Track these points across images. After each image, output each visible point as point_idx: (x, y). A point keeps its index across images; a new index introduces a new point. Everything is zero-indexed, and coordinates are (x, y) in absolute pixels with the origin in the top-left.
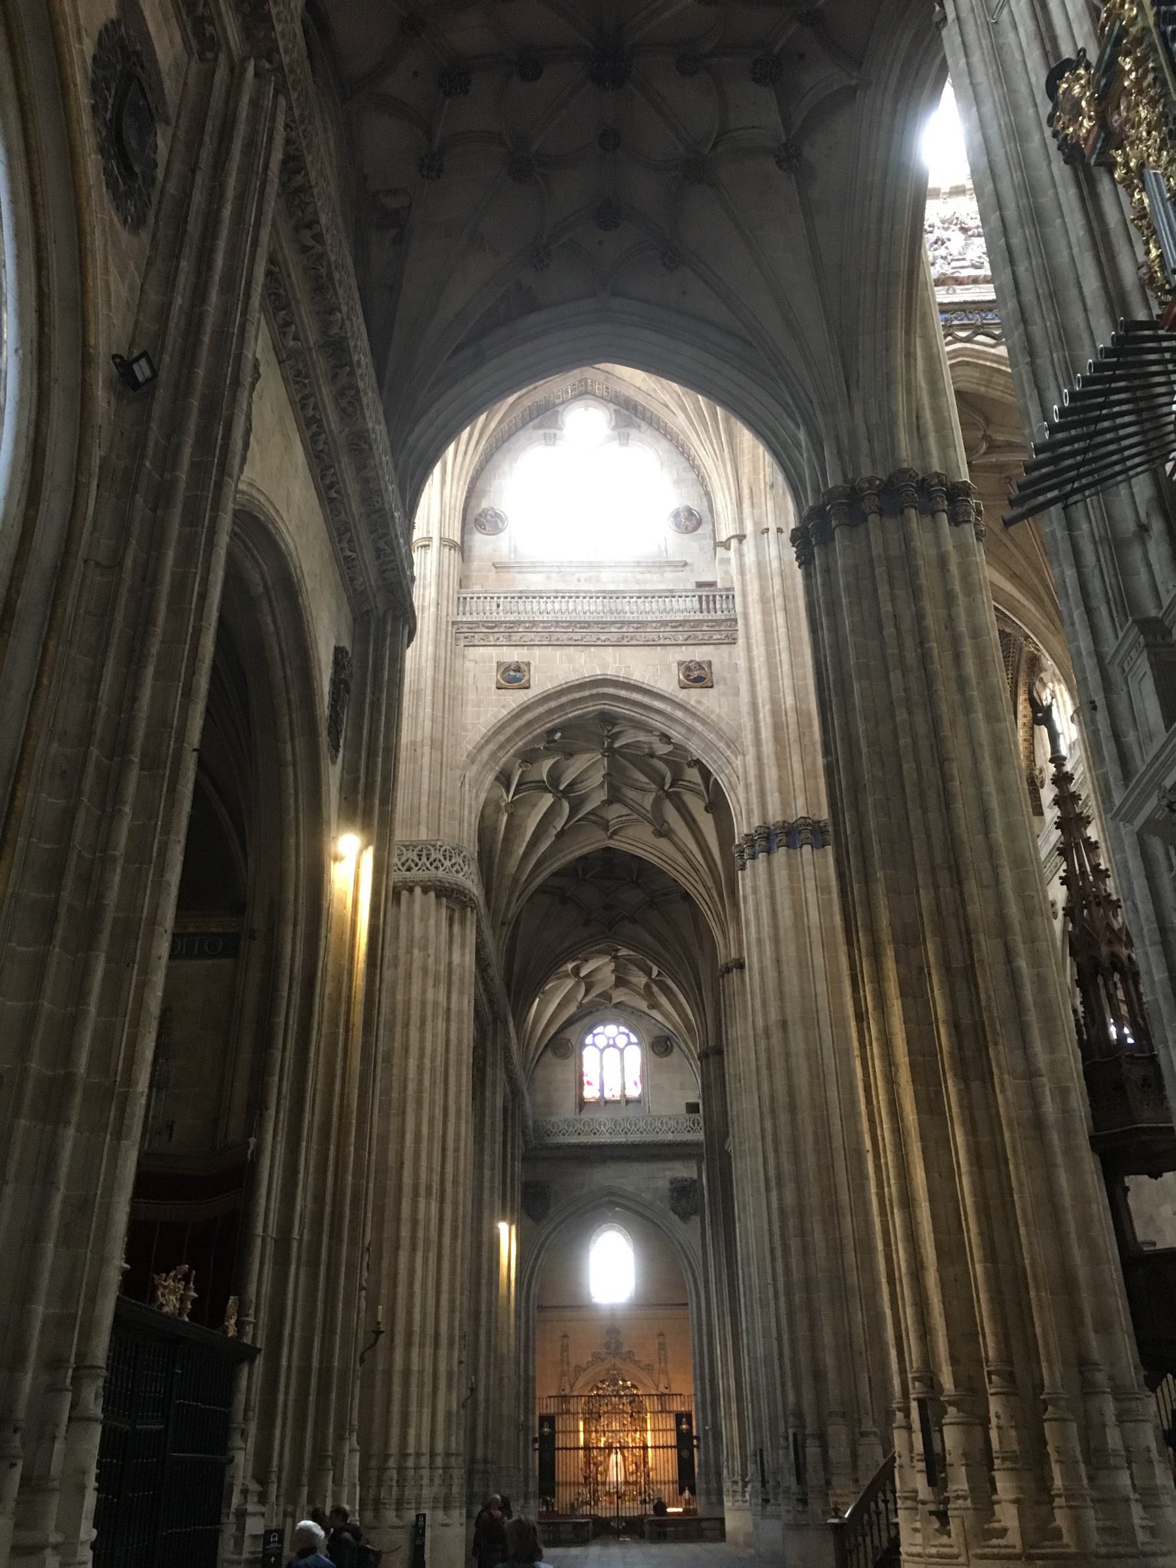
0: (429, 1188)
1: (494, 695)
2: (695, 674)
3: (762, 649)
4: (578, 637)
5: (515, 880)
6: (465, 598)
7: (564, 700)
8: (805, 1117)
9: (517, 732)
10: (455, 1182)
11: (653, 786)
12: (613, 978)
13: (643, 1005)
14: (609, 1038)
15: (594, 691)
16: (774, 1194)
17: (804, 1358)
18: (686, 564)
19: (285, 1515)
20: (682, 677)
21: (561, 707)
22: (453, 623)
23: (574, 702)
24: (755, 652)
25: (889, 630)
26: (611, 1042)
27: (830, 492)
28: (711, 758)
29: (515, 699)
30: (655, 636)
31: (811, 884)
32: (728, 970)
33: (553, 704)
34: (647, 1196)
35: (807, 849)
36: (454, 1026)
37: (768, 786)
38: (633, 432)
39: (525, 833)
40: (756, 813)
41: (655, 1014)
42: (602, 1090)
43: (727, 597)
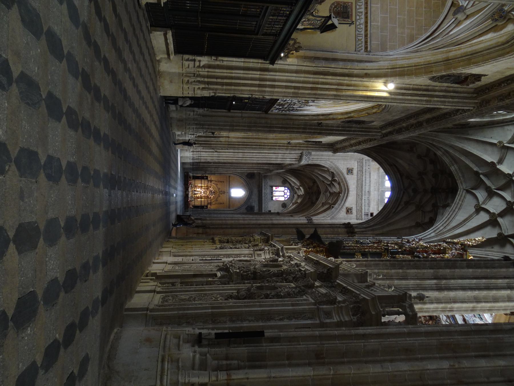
0: (244, 155)
1: (345, 167)
2: (349, 211)
10: (245, 160)
12: (300, 194)
13: (293, 201)
14: (286, 193)
15: (346, 189)
16: (242, 219)
21: (343, 182)
23: (344, 185)
29: (345, 171)
33: (344, 180)
36: (274, 159)
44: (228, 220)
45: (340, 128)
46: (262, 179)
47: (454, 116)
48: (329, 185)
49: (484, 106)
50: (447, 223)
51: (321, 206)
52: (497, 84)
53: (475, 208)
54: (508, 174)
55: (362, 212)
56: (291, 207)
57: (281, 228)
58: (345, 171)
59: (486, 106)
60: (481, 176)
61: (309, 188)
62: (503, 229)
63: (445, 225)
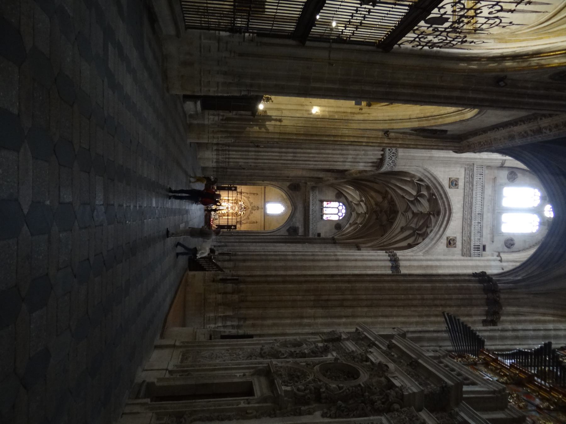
0: (295, 157)
1: (447, 177)
2: (452, 242)
4: (467, 204)
5: (389, 182)
6: (483, 168)
7: (445, 199)
9: (434, 184)
10: (297, 164)
11: (417, 227)
12: (360, 212)
13: (351, 221)
14: (341, 210)
15: (447, 209)
16: (291, 253)
17: (249, 257)
18: (493, 242)
19: (218, 125)
20: (451, 238)
22: (474, 164)
23: (444, 202)
24: (458, 262)
26: (340, 211)
28: (423, 245)
29: (446, 184)
30: (466, 230)
33: (443, 196)
34: (294, 220)
36: (341, 163)
38: (546, 227)
39: (404, 186)
40: (403, 258)
42: (326, 207)
43: (479, 255)
46: (309, 192)
48: (412, 202)
51: (399, 232)
56: (347, 229)
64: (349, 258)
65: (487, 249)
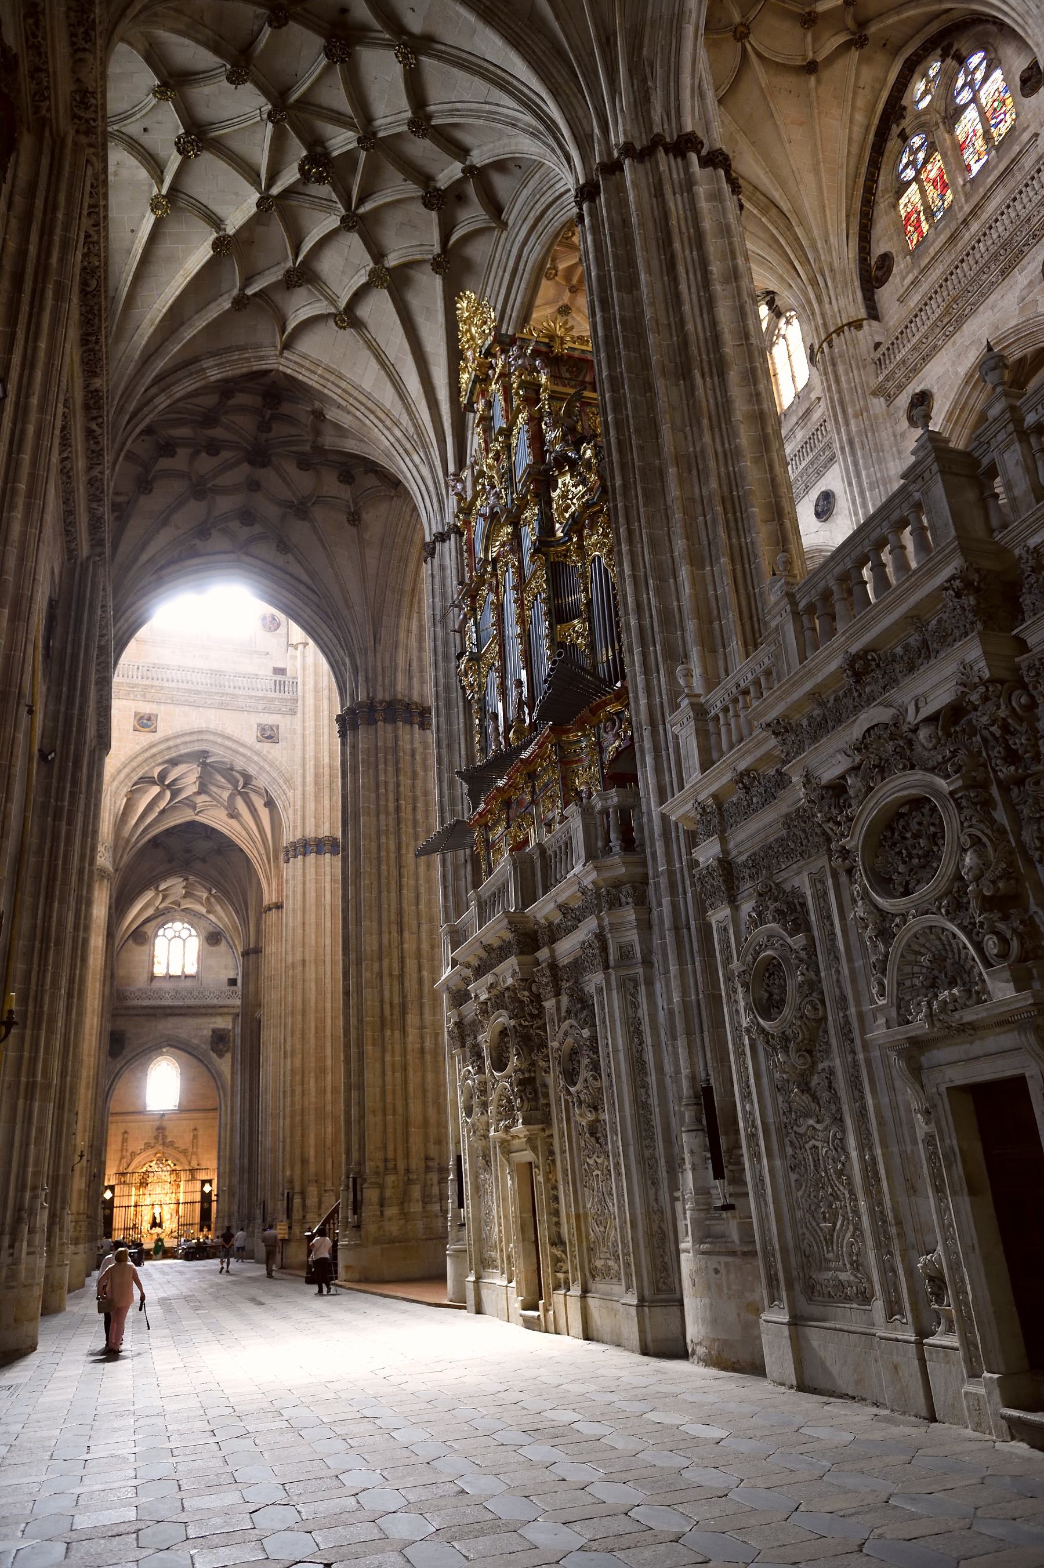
2: (268, 733)
3: (312, 723)
5: (128, 841)
8: (312, 1017)
13: (203, 910)
16: (289, 1060)
17: (298, 1152)
25: (382, 791)
27: (358, 704)
29: (145, 738)
31: (328, 878)
32: (270, 909)
34: (196, 1041)
35: (328, 855)
37: (307, 813)
40: (299, 830)
41: (211, 917)
44: (293, 1104)
45: (65, 689)
46: (128, 1008)
47: (99, 256)
48: (174, 795)
49: (95, 120)
50: (383, 416)
52: (31, 21)
53: (344, 328)
54: (258, 205)
55: (273, 699)
57: (358, 922)
58: (145, 738)
59: (96, 112)
60: (250, 292)
61: (171, 860)
62: (419, 257)
63: (388, 423)
64: (299, 938)
65: (281, 665)
